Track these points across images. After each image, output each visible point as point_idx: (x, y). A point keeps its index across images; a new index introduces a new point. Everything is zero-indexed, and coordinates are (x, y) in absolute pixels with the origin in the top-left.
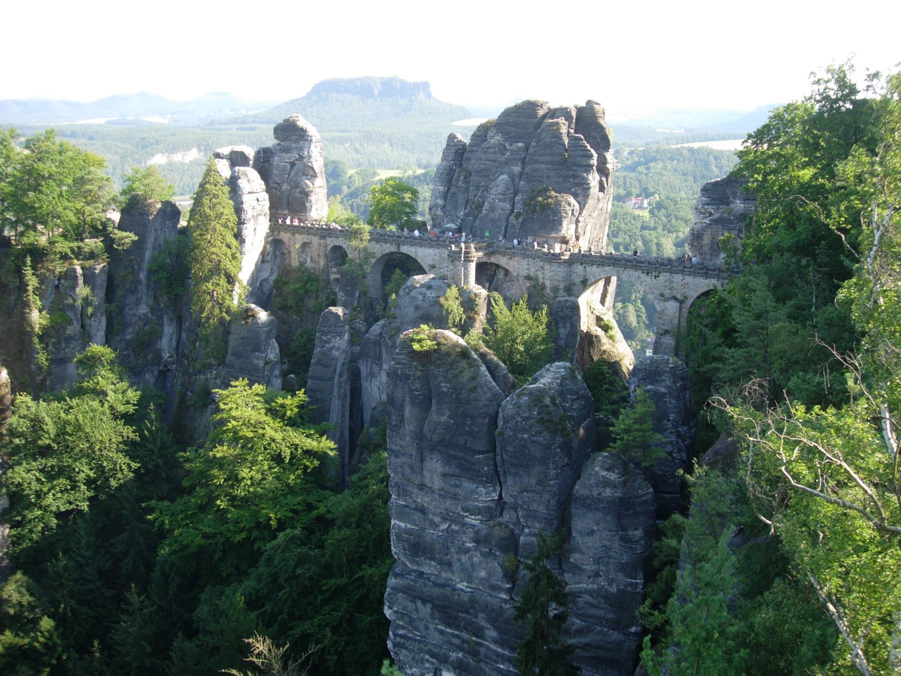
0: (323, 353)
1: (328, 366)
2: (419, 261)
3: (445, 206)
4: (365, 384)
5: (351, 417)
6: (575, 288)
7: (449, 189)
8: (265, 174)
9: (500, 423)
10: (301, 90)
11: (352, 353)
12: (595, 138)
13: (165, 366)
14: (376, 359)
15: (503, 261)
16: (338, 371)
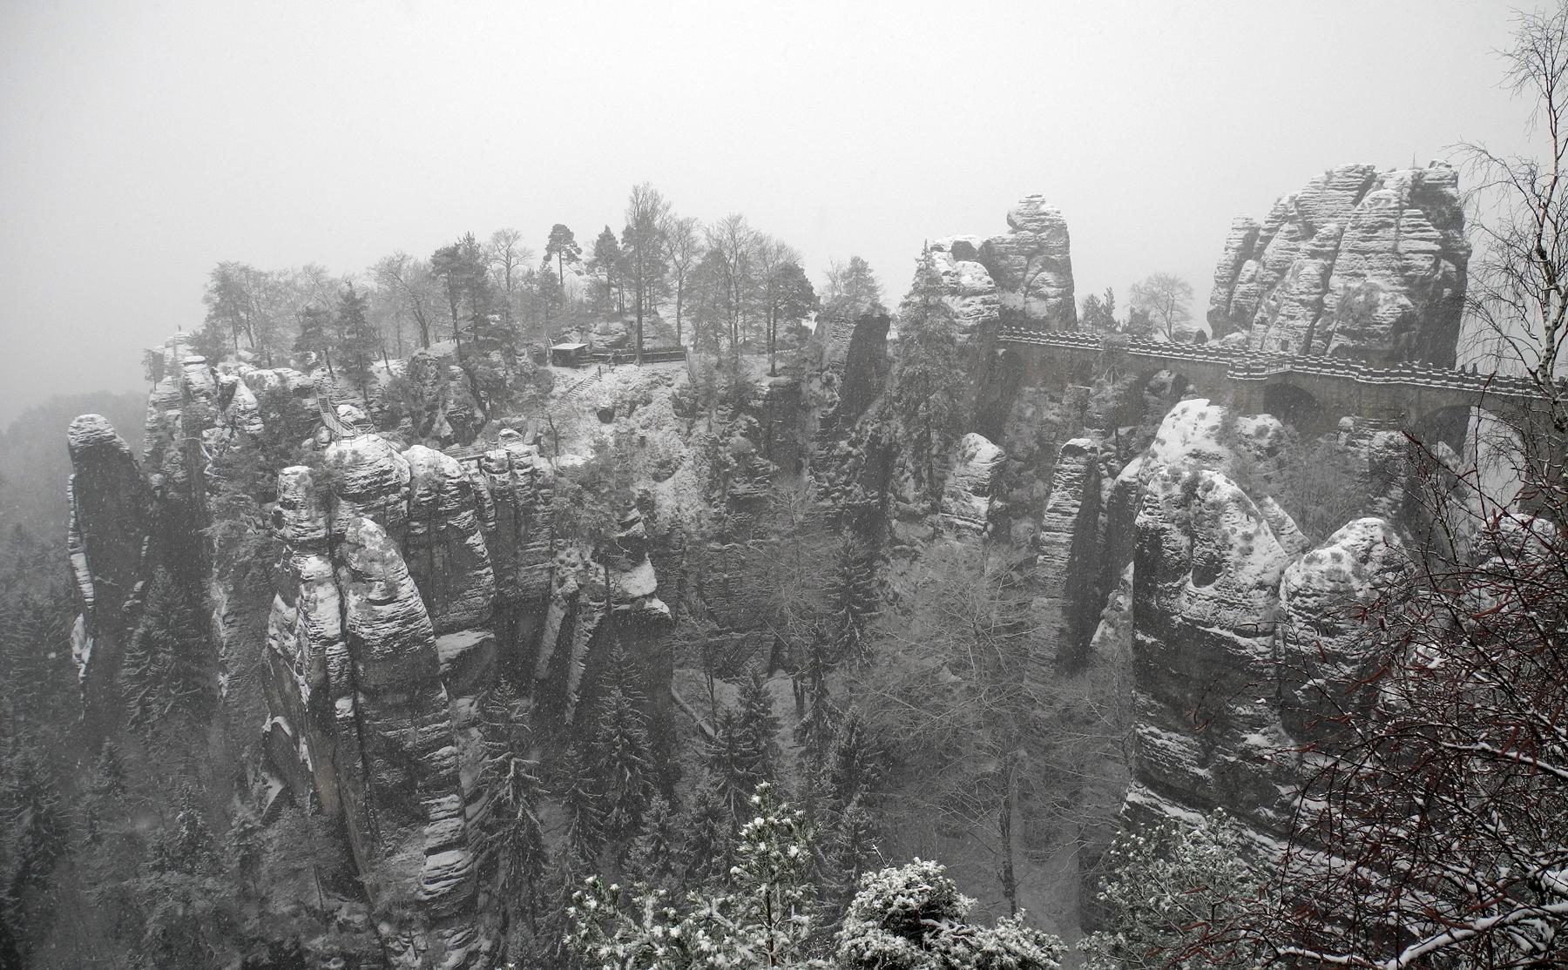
12: (1441, 214)
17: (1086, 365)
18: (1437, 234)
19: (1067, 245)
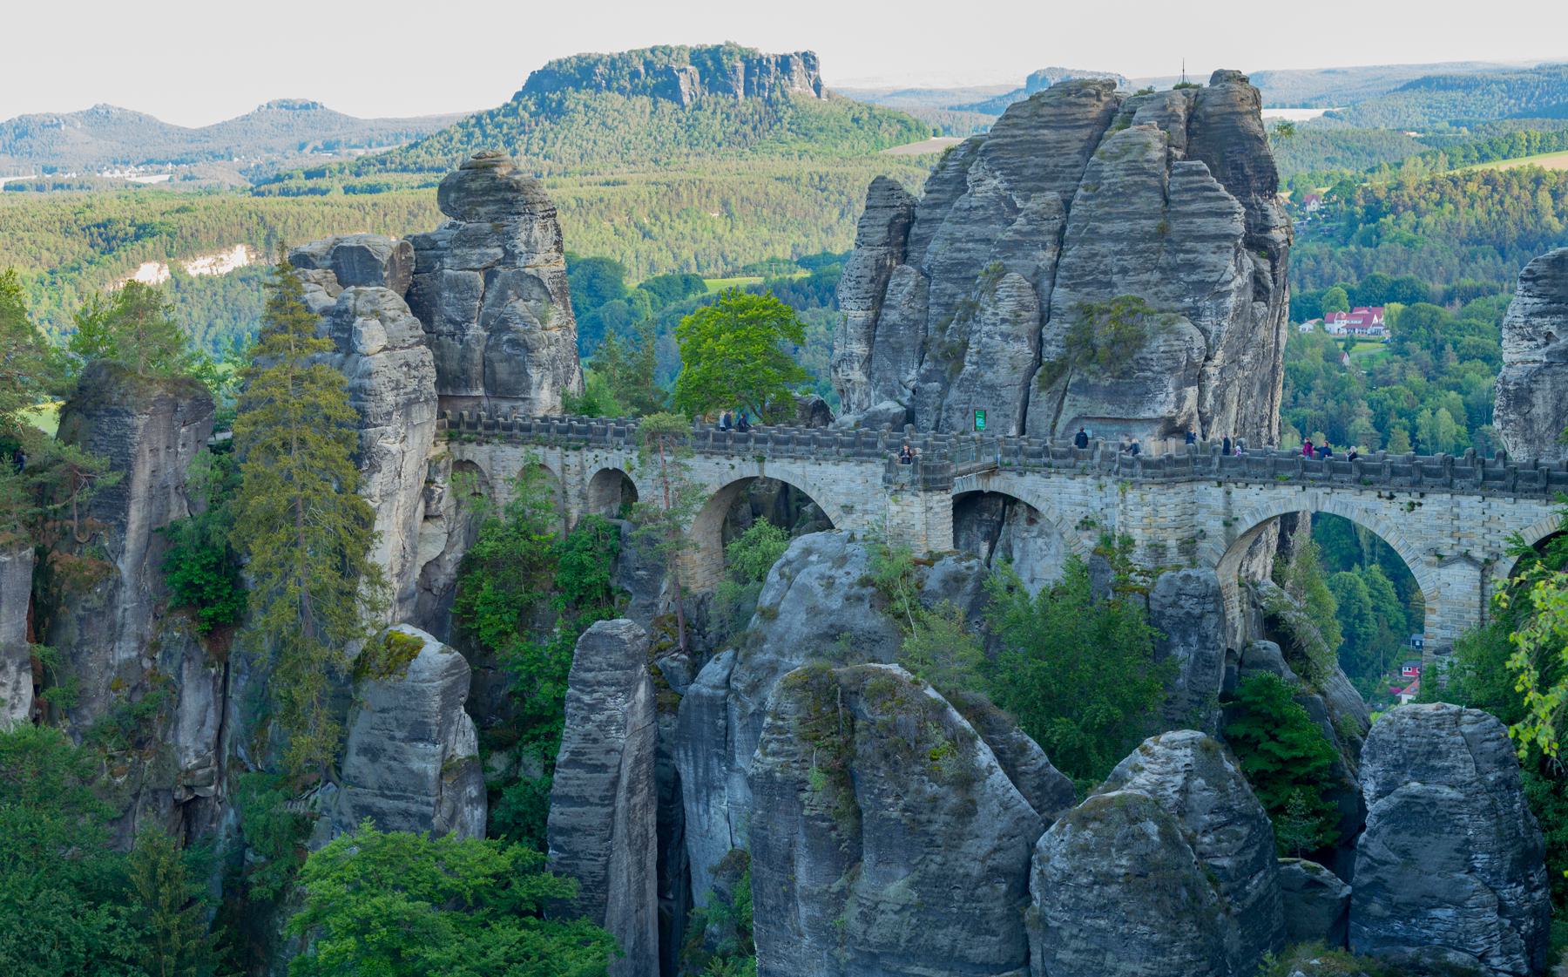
0: (586, 737)
1: (603, 768)
2: (813, 495)
3: (869, 359)
4: (691, 807)
5: (661, 894)
6: (1204, 545)
7: (877, 315)
8: (419, 302)
10: (496, 88)
11: (660, 739)
12: (1238, 167)
13: (189, 788)
14: (717, 745)
15: (1022, 486)
16: (624, 781)
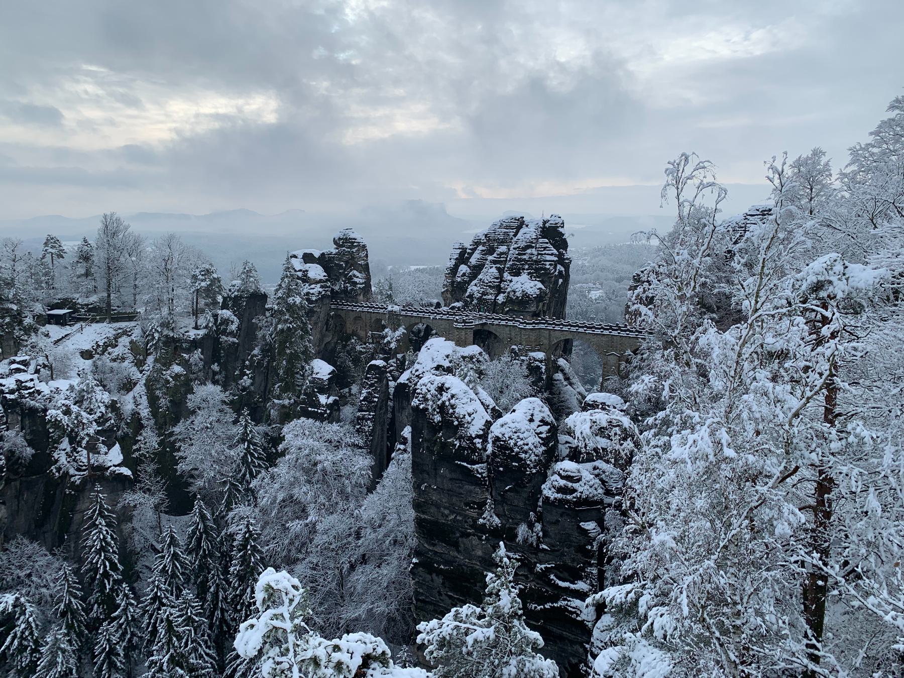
9: (490, 441)
17: (379, 321)
18: (555, 252)
19: (367, 256)
